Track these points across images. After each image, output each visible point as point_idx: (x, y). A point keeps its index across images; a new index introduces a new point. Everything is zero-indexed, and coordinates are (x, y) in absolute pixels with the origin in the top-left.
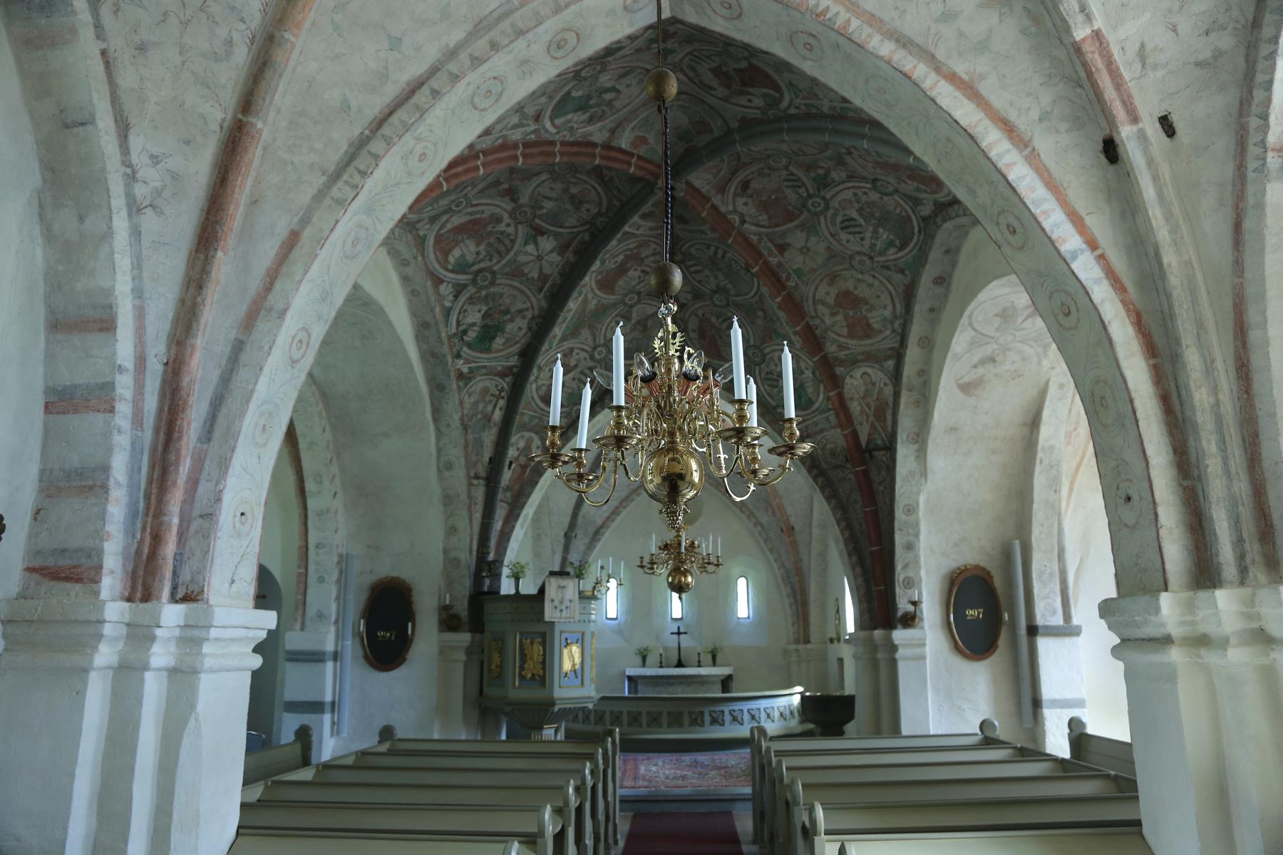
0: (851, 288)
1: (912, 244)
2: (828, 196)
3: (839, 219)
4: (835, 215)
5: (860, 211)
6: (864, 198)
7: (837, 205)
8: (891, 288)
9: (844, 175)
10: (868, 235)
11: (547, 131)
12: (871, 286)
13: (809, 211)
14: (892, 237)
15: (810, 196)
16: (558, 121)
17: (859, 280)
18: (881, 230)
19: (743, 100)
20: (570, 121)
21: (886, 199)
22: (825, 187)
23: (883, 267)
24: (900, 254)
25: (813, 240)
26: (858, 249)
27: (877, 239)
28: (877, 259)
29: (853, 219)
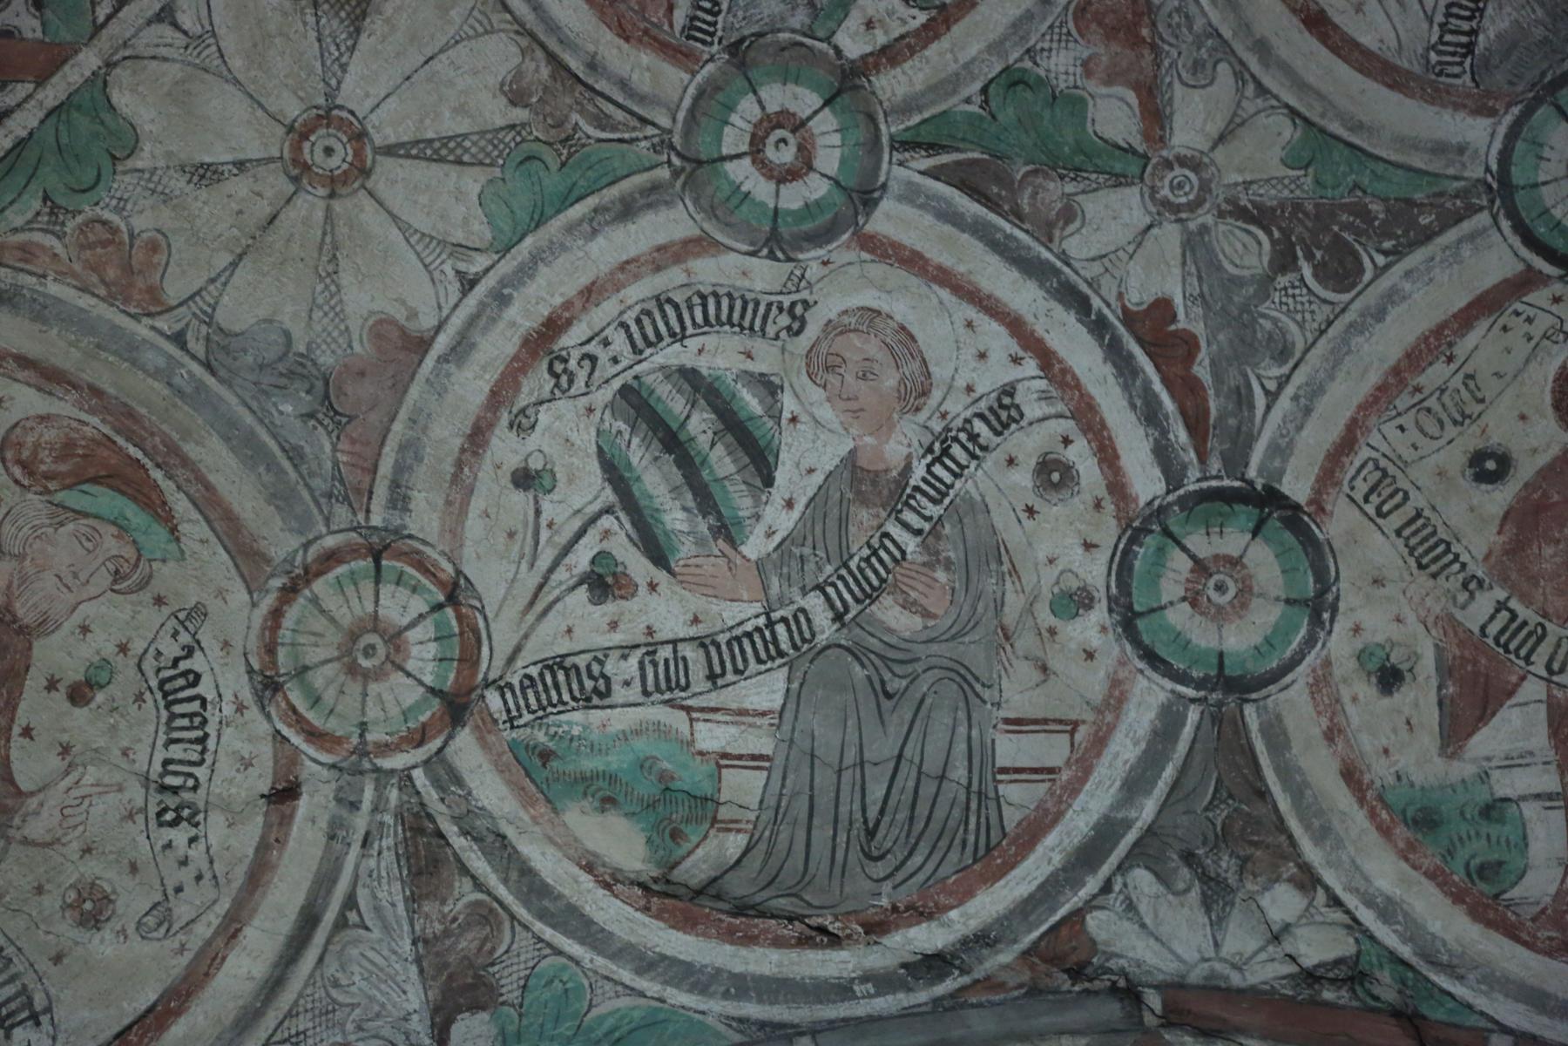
0: (58, 655)
1: (763, 961)
2: (891, 219)
3: (719, 354)
4: (736, 313)
5: (858, 479)
6: (999, 482)
7: (830, 305)
8: (244, 968)
9: (1158, 276)
10: (665, 610)
12: (175, 804)
13: (709, 105)
14: (743, 787)
15: (847, 84)
17: (176, 688)
18: (765, 690)
21: (1093, 627)
22: (966, 179)
23: (418, 824)
24: (613, 913)
25: (456, 202)
26: (495, 579)
27: (667, 684)
28: (465, 748)
29: (760, 462)
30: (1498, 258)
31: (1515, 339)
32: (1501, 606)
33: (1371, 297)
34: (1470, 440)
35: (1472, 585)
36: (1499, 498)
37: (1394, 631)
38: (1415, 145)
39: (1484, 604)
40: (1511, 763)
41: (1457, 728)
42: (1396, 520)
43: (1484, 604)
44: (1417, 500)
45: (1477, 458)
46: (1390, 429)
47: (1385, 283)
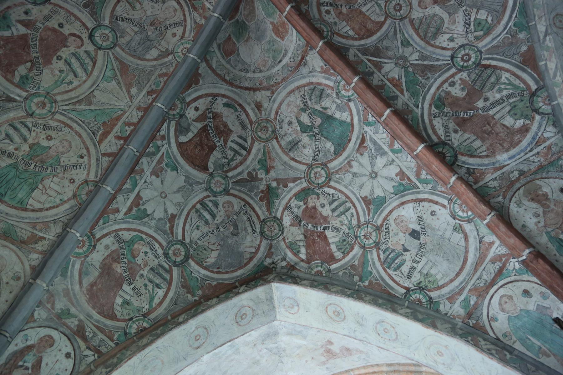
11: (358, 113)
16: (344, 116)
19: (202, 104)
20: (338, 107)
30: (90, 25)
31: (80, 28)
32: (41, 28)
33: (82, 10)
34: (64, 23)
35: (43, 24)
36: (56, 27)
37: (34, 13)
38: (104, 14)
39: (41, 25)
40: (17, 29)
41: (21, 22)
42: (51, 14)
43: (41, 25)
44: (54, 16)
45: (62, 24)
46: (64, 13)
47: (85, 12)
